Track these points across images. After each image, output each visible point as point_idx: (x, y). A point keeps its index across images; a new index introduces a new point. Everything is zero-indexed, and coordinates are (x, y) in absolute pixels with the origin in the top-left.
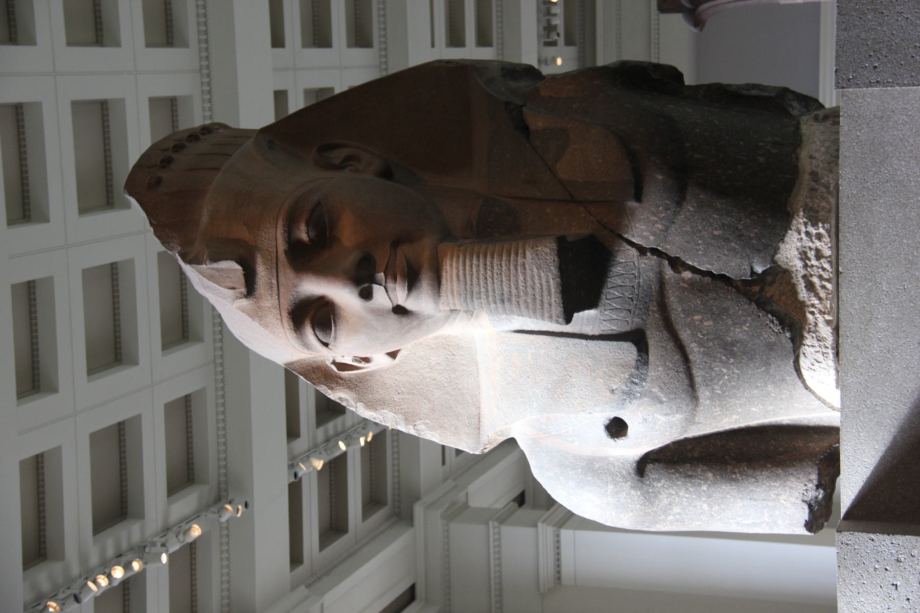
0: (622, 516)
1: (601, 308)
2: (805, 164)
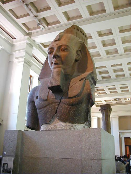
2: (74, 125)
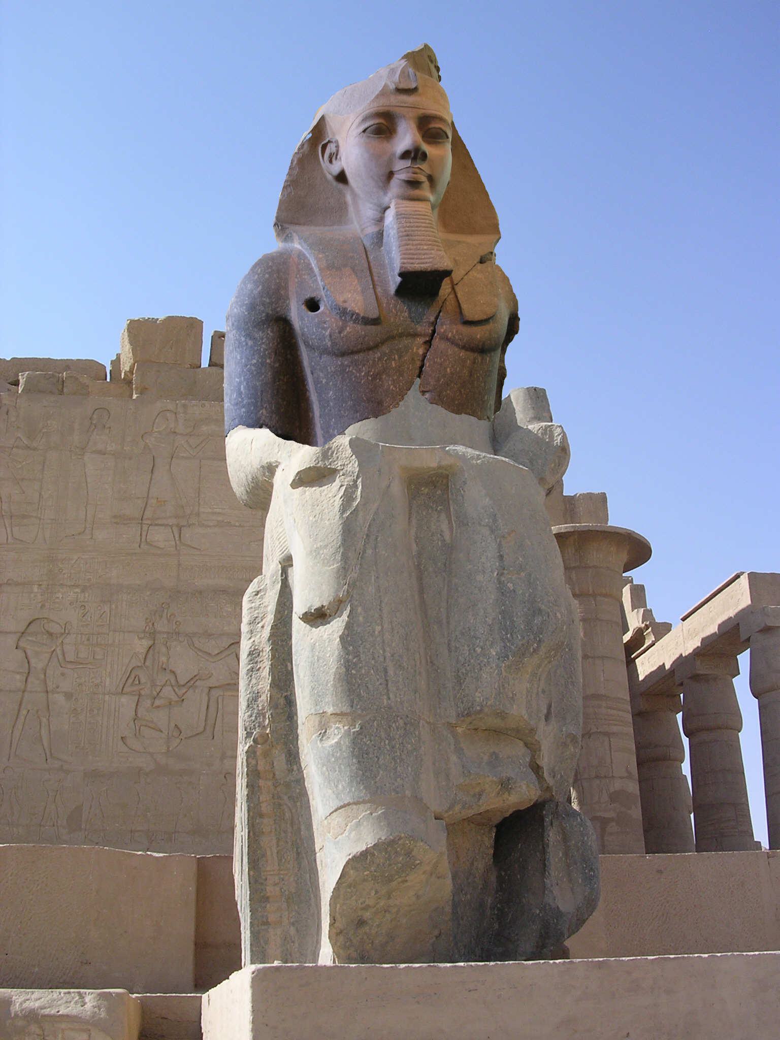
1: (395, 298)
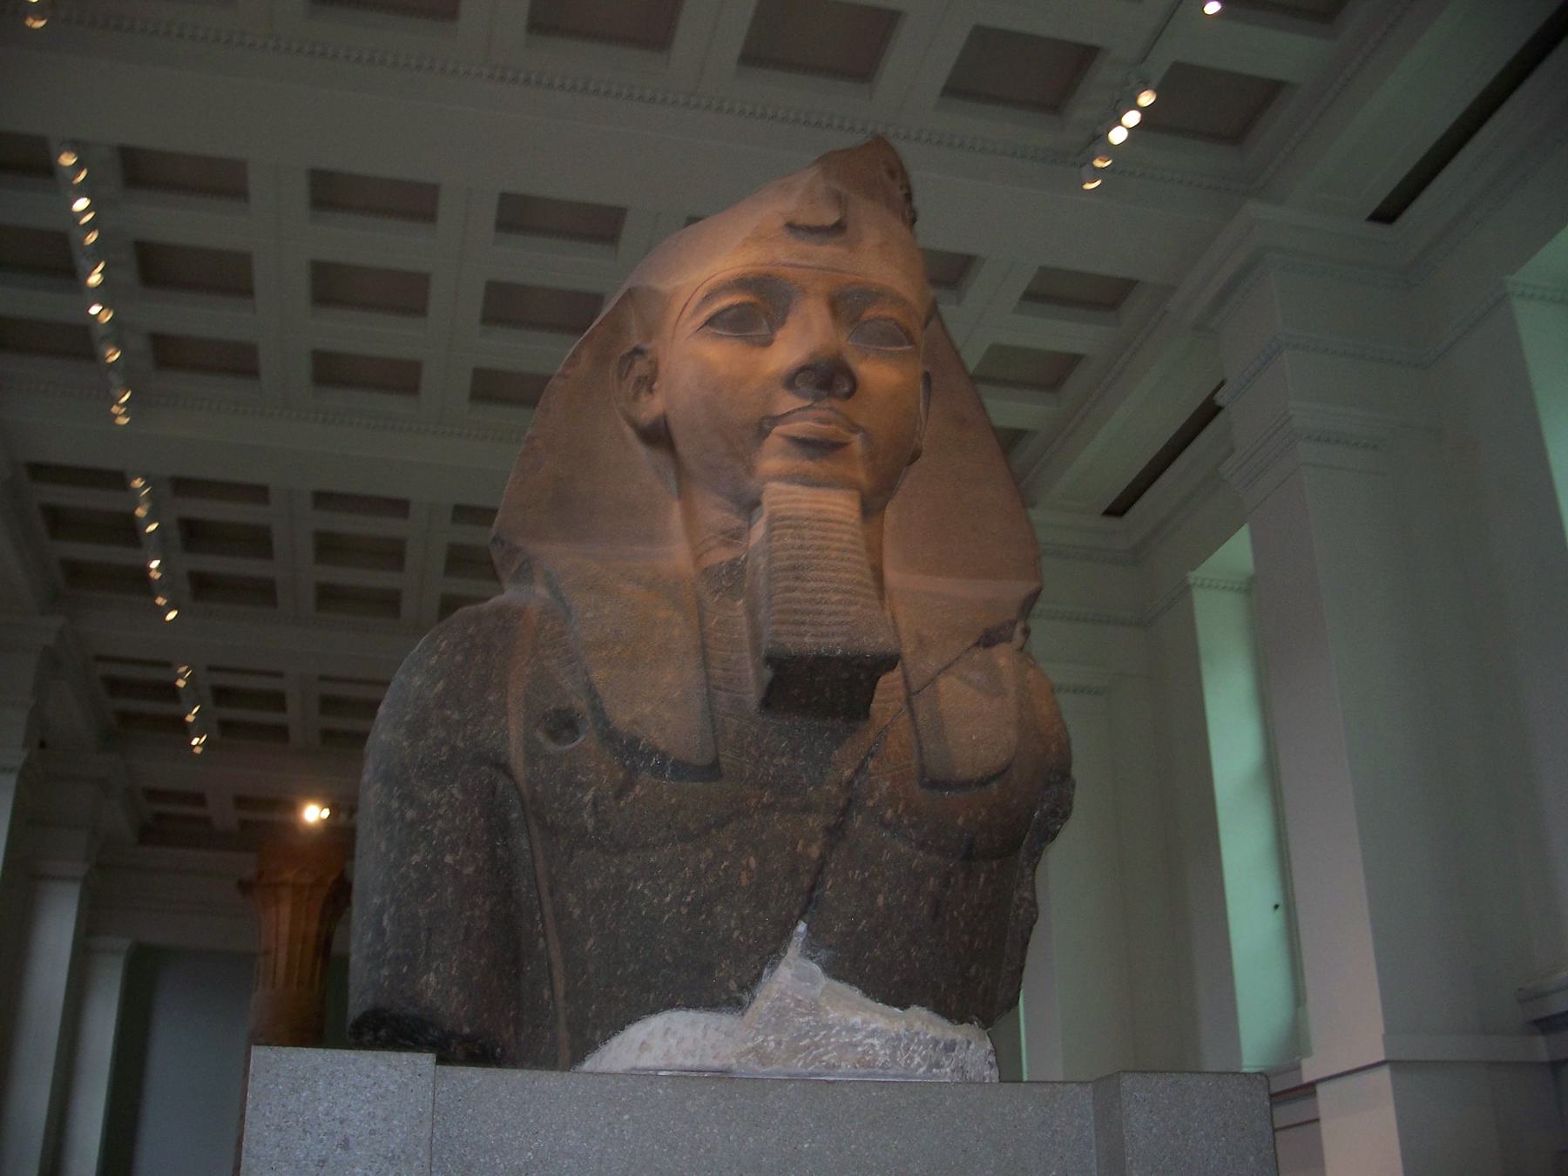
0: (402, 730)
